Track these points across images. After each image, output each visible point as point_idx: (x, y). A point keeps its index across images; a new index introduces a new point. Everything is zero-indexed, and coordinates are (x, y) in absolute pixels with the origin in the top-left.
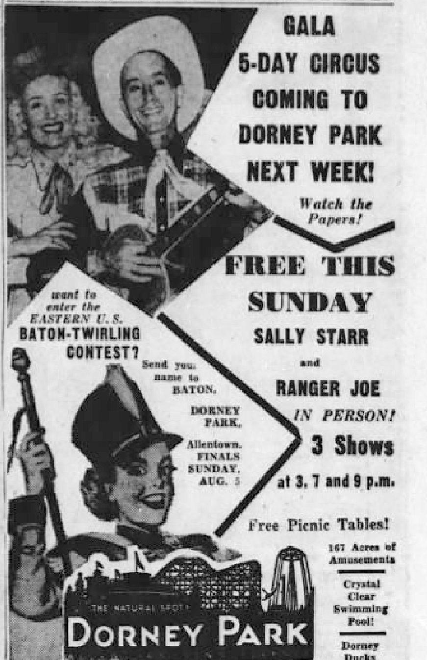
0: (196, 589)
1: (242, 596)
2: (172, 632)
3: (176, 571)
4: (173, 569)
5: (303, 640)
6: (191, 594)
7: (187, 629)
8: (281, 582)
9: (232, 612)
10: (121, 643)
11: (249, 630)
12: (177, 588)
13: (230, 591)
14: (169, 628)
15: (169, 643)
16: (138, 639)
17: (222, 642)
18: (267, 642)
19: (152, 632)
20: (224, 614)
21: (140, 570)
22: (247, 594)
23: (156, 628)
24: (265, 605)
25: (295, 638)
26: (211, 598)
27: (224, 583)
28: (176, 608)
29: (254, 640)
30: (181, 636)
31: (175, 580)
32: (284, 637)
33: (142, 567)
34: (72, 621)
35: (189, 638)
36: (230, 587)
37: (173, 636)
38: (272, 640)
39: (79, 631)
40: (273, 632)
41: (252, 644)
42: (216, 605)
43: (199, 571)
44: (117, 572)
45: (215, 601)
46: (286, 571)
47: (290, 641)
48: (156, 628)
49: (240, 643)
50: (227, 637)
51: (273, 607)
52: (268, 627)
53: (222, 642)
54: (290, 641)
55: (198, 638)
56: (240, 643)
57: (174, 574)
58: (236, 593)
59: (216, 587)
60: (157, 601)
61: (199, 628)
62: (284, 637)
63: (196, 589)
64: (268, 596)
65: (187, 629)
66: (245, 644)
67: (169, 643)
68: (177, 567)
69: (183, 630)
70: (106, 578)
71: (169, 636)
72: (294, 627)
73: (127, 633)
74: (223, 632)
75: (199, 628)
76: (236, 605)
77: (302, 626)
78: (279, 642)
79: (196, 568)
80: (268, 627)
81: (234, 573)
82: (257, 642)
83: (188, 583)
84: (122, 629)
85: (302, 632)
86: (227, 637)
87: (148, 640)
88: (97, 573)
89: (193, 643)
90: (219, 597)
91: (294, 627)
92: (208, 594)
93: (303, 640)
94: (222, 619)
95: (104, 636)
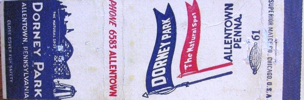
2: (38, 44)
3: (67, 45)
4: (68, 44)
5: (36, 95)
15: (34, 43)
18: (35, 81)
21: (67, 31)
30: (37, 48)
32: (37, 88)
33: (68, 32)
35: (36, 51)
37: (37, 45)
38: (36, 83)
40: (39, 84)
41: (34, 76)
43: (67, 55)
44: (67, 22)
47: (36, 90)
49: (35, 70)
50: (37, 65)
54: (36, 90)
55: (36, 55)
56: (35, 70)
57: (66, 44)
62: (37, 88)
66: (34, 72)
67: (34, 43)
68: (68, 46)
69: (39, 48)
70: (65, 18)
71: (37, 42)
74: (38, 64)
78: (35, 86)
79: (68, 53)
81: (66, 69)
82: (35, 77)
85: (39, 95)
86: (37, 65)
87: (35, 34)
88: (66, 14)
89: (35, 52)
93: (36, 95)
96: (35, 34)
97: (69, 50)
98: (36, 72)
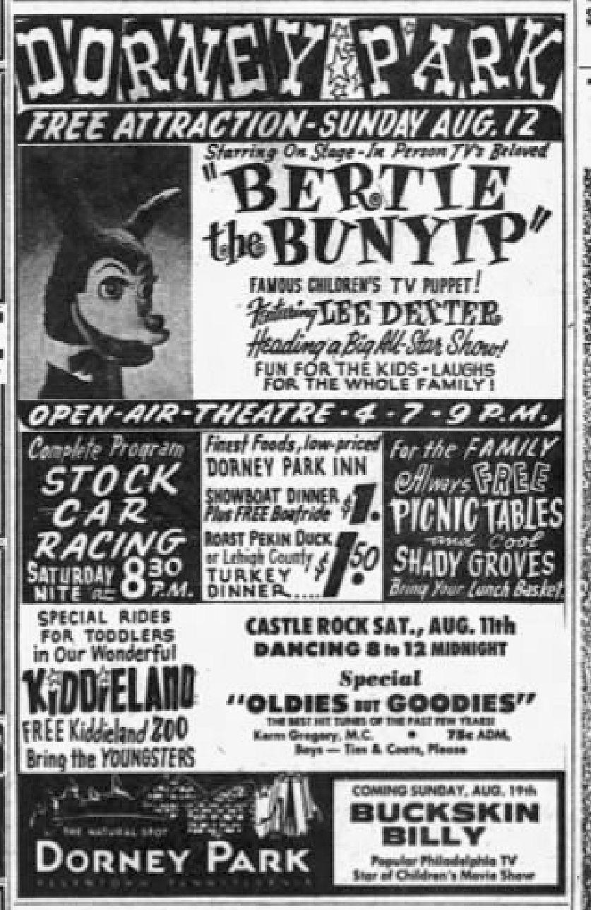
0: (182, 812)
1: (235, 820)
2: (155, 857)
3: (159, 792)
5: (304, 868)
6: (177, 819)
7: (172, 853)
8: (278, 807)
9: (225, 837)
10: (96, 869)
11: (242, 856)
12: (159, 811)
13: (221, 815)
14: (151, 854)
15: (151, 869)
16: (116, 864)
17: (211, 868)
18: (263, 869)
19: (131, 855)
20: (214, 839)
22: (240, 817)
23: (137, 853)
24: (261, 831)
25: (296, 867)
26: (198, 822)
27: (214, 805)
28: (160, 832)
29: (248, 866)
30: (166, 862)
31: (158, 802)
32: (283, 863)
34: (41, 845)
36: (221, 811)
37: (157, 862)
38: (268, 867)
39: (49, 856)
40: (270, 858)
42: (205, 829)
45: (204, 825)
46: (283, 794)
47: (290, 868)
48: (137, 853)
49: (232, 869)
50: (218, 865)
51: (271, 833)
52: (264, 853)
53: (211, 868)
54: (290, 868)
55: (185, 864)
56: (232, 869)
57: (158, 796)
58: (227, 817)
59: (204, 810)
60: (138, 825)
61: (186, 853)
62: (283, 863)
63: (182, 812)
64: (264, 820)
65: (172, 853)
66: (237, 872)
67: (151, 869)
71: (151, 862)
72: (295, 853)
73: (103, 859)
74: (213, 859)
75: (186, 853)
76: (228, 831)
77: (302, 853)
79: (182, 789)
80: (264, 853)
83: (173, 806)
84: (97, 854)
85: (304, 859)
86: (218, 865)
87: (127, 866)
89: (179, 869)
90: (209, 821)
91: (295, 853)
92: (196, 817)
93: (304, 868)
94: (212, 845)
95: (77, 862)
96: (127, 866)
97: (172, 786)
98: (235, 867)
